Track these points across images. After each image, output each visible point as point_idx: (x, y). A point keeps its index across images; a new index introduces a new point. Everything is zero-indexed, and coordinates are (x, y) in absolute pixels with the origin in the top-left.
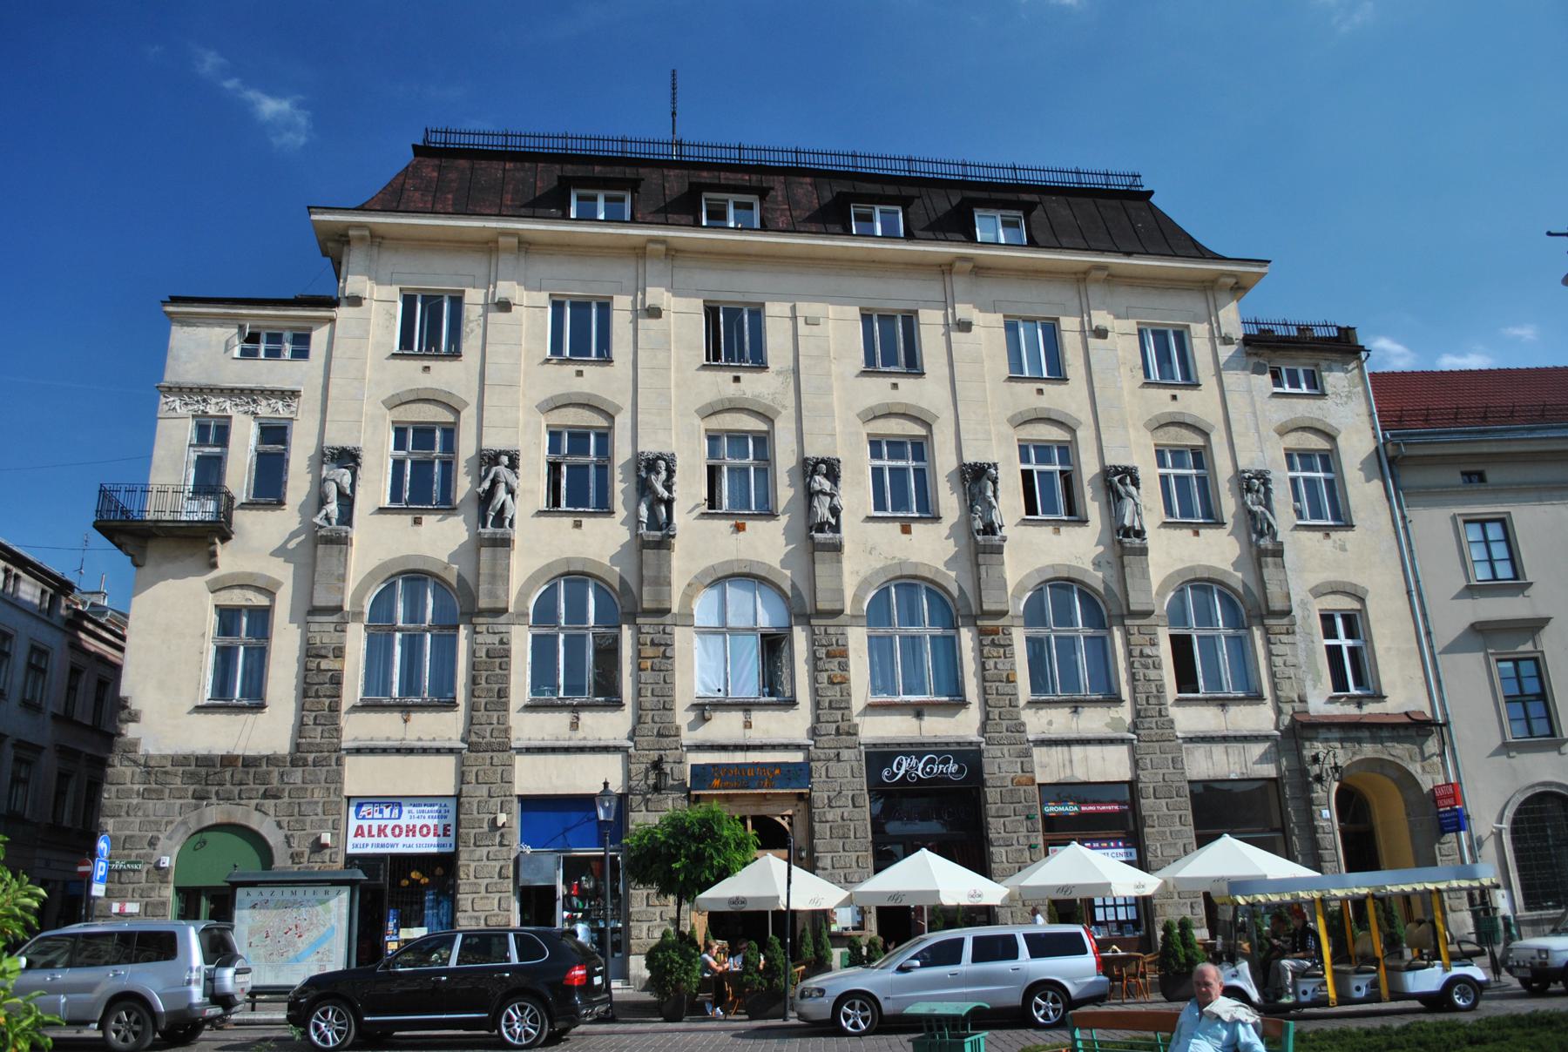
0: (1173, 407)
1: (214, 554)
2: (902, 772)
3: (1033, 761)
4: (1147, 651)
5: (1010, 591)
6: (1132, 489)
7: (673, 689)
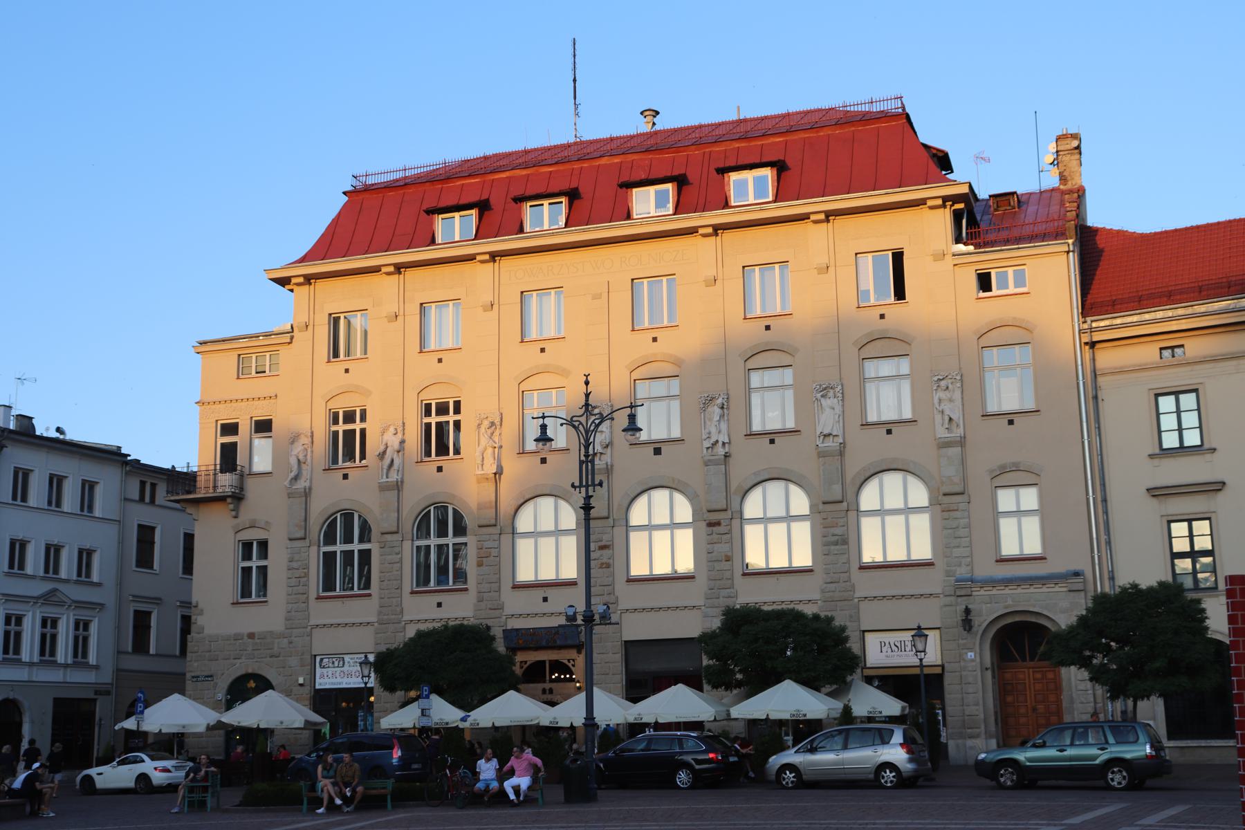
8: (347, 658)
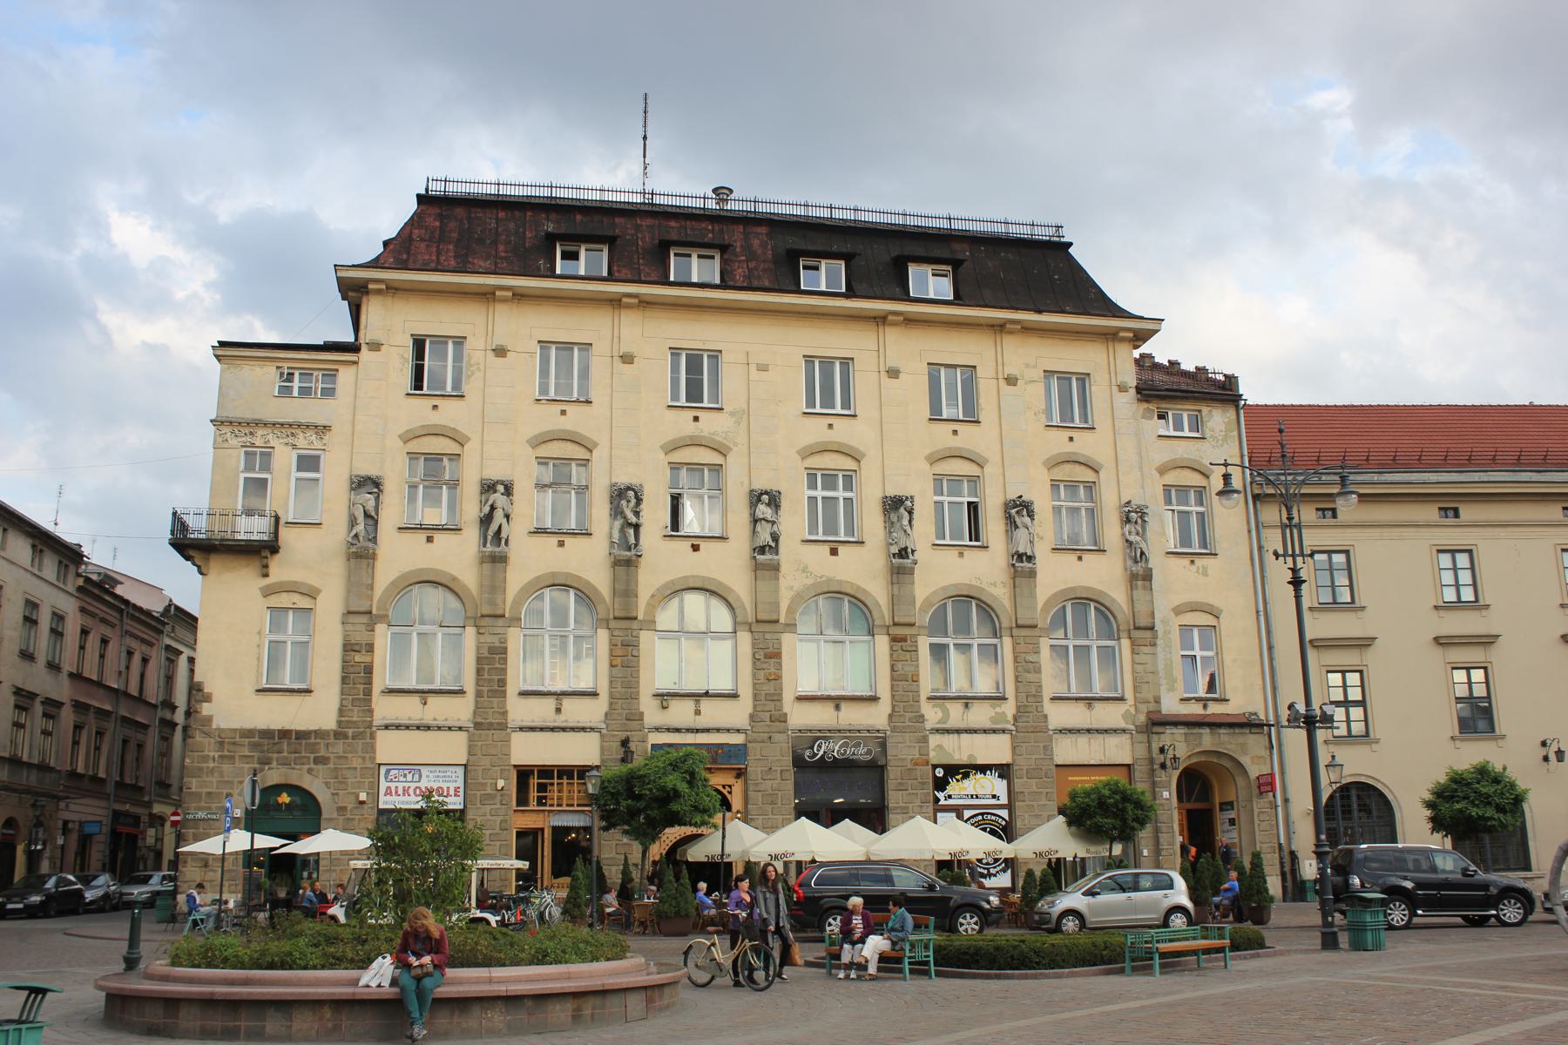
0: (1069, 448)
1: (266, 566)
2: (821, 753)
3: (928, 747)
4: (1030, 658)
5: (918, 606)
6: (1027, 520)
7: (638, 682)
8: (425, 771)
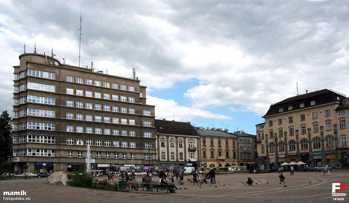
0: (328, 119)
